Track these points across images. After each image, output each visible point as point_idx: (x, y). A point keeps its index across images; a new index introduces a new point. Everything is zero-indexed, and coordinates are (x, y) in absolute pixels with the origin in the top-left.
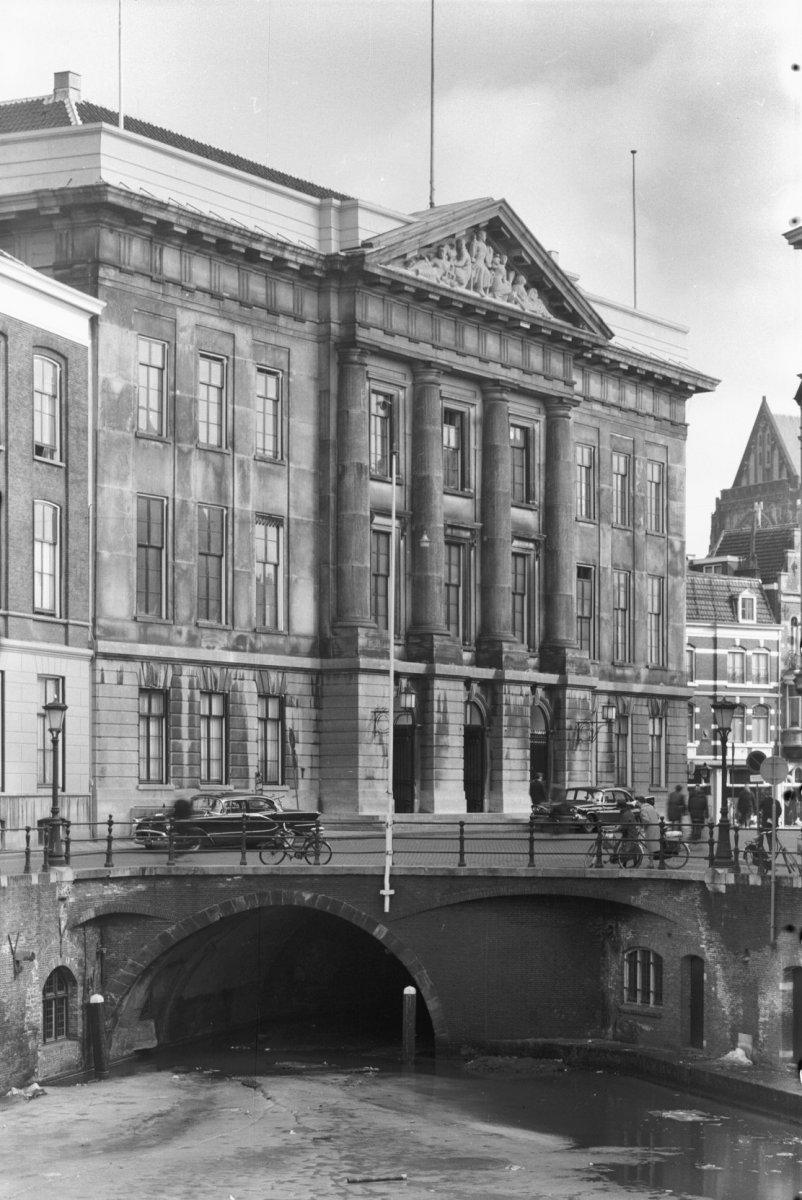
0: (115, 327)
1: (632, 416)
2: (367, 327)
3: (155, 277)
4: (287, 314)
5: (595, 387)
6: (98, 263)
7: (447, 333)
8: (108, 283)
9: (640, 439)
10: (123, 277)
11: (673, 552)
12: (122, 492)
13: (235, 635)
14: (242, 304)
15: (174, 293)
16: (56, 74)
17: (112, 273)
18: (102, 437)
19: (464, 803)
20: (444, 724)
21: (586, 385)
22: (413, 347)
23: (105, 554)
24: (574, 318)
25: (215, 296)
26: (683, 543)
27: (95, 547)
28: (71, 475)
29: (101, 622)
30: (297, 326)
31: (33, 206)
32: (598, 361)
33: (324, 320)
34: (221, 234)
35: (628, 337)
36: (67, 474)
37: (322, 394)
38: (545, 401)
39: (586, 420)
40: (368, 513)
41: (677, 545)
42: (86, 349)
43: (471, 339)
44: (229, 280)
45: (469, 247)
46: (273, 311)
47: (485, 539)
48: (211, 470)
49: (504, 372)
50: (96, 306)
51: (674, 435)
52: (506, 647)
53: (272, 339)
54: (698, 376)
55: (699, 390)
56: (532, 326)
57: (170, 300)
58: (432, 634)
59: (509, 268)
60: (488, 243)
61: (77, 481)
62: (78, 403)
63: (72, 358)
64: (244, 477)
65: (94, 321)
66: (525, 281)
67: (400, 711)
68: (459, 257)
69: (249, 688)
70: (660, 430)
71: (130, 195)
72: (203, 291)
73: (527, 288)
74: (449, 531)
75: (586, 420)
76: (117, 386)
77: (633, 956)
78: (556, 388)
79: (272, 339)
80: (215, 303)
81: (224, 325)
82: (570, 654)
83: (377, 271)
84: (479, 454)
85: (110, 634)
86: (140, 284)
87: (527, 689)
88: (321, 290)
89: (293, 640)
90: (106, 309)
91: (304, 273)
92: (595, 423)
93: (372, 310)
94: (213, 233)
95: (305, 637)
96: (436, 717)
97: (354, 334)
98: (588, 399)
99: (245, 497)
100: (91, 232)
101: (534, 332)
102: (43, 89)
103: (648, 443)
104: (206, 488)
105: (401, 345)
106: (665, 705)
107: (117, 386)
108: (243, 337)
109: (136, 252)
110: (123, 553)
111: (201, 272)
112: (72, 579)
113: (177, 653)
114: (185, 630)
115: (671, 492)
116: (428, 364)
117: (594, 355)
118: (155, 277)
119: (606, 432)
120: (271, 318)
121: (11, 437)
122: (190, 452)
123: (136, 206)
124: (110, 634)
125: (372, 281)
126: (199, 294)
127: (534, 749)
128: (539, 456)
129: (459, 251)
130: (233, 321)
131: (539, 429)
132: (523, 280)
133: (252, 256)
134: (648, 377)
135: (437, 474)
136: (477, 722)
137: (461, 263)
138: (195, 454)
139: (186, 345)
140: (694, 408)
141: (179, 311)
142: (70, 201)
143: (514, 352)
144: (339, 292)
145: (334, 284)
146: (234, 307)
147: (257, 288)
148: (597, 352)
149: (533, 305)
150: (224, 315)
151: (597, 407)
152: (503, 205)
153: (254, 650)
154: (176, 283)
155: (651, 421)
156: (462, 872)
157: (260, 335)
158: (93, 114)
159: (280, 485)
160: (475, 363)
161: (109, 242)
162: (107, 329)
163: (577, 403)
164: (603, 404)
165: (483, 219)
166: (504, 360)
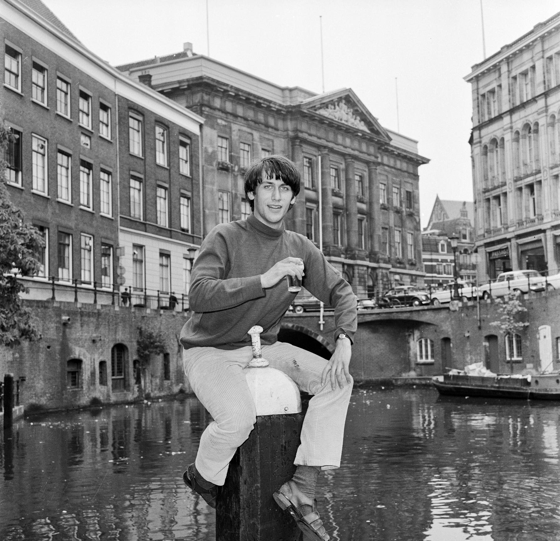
1: (399, 172)
4: (272, 128)
5: (386, 160)
7: (331, 136)
8: (206, 113)
10: (211, 111)
11: (417, 222)
12: (213, 189)
15: (231, 118)
17: (207, 109)
18: (205, 168)
21: (382, 159)
23: (207, 211)
24: (377, 133)
25: (246, 119)
26: (419, 219)
27: (203, 208)
28: (194, 181)
30: (276, 132)
31: (177, 86)
32: (386, 150)
34: (247, 96)
39: (383, 172)
41: (418, 220)
42: (198, 136)
43: (340, 139)
44: (250, 114)
45: (338, 105)
46: (267, 126)
50: (202, 120)
53: (267, 136)
54: (423, 158)
55: (424, 163)
56: (363, 135)
59: (353, 114)
60: (345, 104)
62: (195, 155)
63: (193, 138)
65: (201, 126)
68: (335, 108)
70: (409, 177)
72: (241, 117)
73: (360, 121)
74: (334, 210)
75: (383, 172)
76: (210, 150)
79: (267, 136)
80: (245, 122)
81: (249, 130)
83: (305, 111)
84: (344, 182)
87: (365, 268)
88: (284, 120)
90: (205, 122)
91: (278, 112)
92: (386, 173)
93: (304, 127)
94: (245, 95)
101: (364, 137)
102: (181, 50)
103: (405, 182)
105: (314, 139)
106: (416, 279)
107: (210, 150)
108: (256, 135)
110: (214, 211)
111: (240, 111)
116: (325, 147)
117: (385, 148)
120: (266, 129)
121: (171, 164)
122: (237, 175)
123: (215, 84)
126: (239, 119)
128: (366, 184)
129: (335, 106)
130: (252, 129)
131: (366, 174)
132: (358, 118)
133: (258, 105)
134: (405, 157)
137: (336, 111)
139: (235, 136)
140: (422, 170)
142: (191, 83)
143: (356, 145)
144: (291, 120)
145: (289, 117)
146: (252, 123)
147: (261, 117)
148: (386, 147)
149: (362, 127)
150: (249, 127)
151: (386, 168)
152: (350, 90)
154: (232, 114)
155: (406, 174)
157: (262, 134)
160: (342, 148)
162: (206, 129)
164: (388, 166)
165: (343, 95)
166: (353, 147)
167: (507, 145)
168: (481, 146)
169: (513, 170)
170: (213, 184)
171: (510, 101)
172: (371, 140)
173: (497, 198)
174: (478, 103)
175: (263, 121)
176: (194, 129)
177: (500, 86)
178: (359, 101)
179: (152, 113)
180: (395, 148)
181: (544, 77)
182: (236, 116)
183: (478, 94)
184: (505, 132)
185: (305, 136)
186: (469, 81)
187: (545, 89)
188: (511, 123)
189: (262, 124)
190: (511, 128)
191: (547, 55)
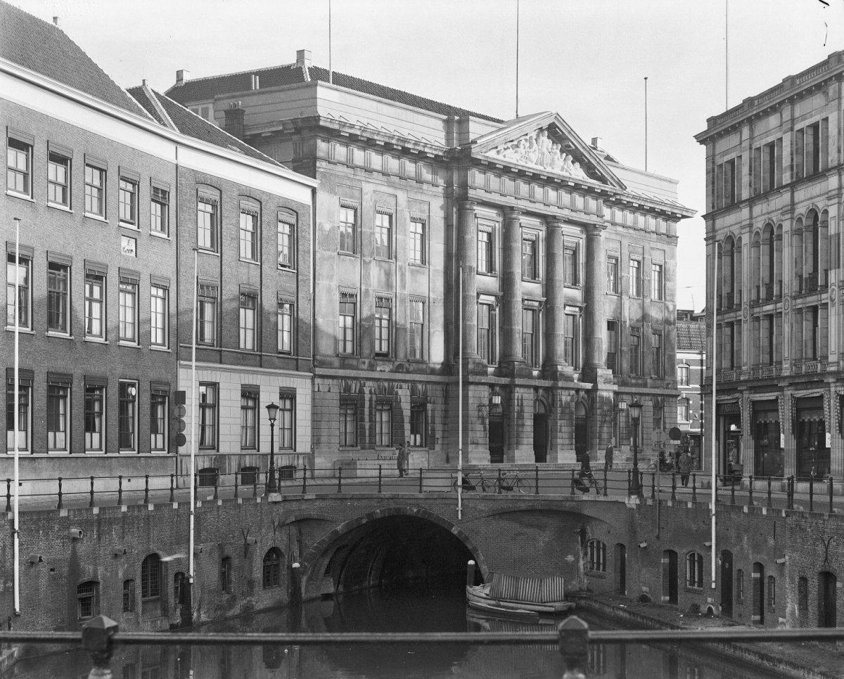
0: (326, 194)
1: (643, 233)
3: (349, 164)
8: (322, 170)
10: (331, 166)
11: (668, 311)
12: (330, 286)
13: (397, 363)
15: (361, 175)
16: (297, 52)
17: (324, 164)
18: (318, 255)
19: (533, 457)
20: (521, 412)
22: (503, 199)
24: (602, 179)
28: (300, 277)
29: (318, 357)
30: (434, 189)
33: (449, 184)
34: (387, 140)
35: (636, 187)
36: (297, 276)
37: (448, 227)
38: (585, 227)
39: (613, 237)
40: (475, 294)
41: (671, 308)
44: (393, 164)
47: (548, 306)
48: (382, 271)
49: (559, 211)
51: (669, 243)
52: (559, 368)
53: (419, 197)
55: (684, 217)
56: (576, 184)
57: (358, 178)
58: (514, 362)
59: (562, 151)
60: (549, 137)
62: (304, 237)
64: (403, 275)
65: (314, 191)
66: (572, 159)
67: (492, 405)
69: (404, 394)
71: (332, 121)
73: (573, 162)
75: (613, 237)
77: (592, 543)
78: (592, 219)
79: (419, 197)
80: (385, 178)
81: (391, 191)
82: (600, 372)
83: (479, 157)
85: (323, 364)
86: (341, 169)
87: (573, 392)
92: (618, 238)
93: (477, 178)
96: (516, 408)
97: (467, 193)
98: (614, 224)
99: (404, 287)
100: (312, 142)
101: (577, 188)
102: (291, 60)
103: (652, 248)
104: (379, 282)
106: (663, 401)
107: (327, 227)
108: (402, 197)
109: (340, 151)
110: (331, 319)
111: (376, 160)
112: (300, 334)
113: (363, 374)
114: (367, 361)
115: (667, 276)
116: (512, 208)
117: (616, 199)
118: (349, 164)
119: (625, 242)
122: (370, 262)
123: (336, 127)
124: (323, 364)
125: (476, 163)
127: (577, 427)
128: (582, 258)
131: (582, 243)
132: (571, 158)
134: (652, 210)
135: (517, 270)
136: (542, 411)
138: (373, 263)
141: (363, 184)
146: (397, 179)
147: (410, 167)
148: (618, 197)
149: (577, 173)
150: (391, 185)
151: (620, 229)
153: (408, 372)
155: (655, 235)
157: (412, 195)
158: (319, 74)
159: (423, 279)
160: (542, 206)
161: (322, 147)
163: (605, 228)
165: (545, 124)
167: (745, 251)
169: (750, 290)
170: (331, 277)
171: (750, 186)
172: (590, 191)
174: (713, 178)
175: (413, 175)
176: (304, 196)
177: (740, 157)
178: (571, 131)
179: (234, 184)
180: (634, 197)
181: (792, 160)
182: (368, 170)
183: (713, 163)
184: (744, 231)
186: (702, 142)
187: (792, 178)
188: (751, 218)
190: (751, 225)
191: (798, 127)
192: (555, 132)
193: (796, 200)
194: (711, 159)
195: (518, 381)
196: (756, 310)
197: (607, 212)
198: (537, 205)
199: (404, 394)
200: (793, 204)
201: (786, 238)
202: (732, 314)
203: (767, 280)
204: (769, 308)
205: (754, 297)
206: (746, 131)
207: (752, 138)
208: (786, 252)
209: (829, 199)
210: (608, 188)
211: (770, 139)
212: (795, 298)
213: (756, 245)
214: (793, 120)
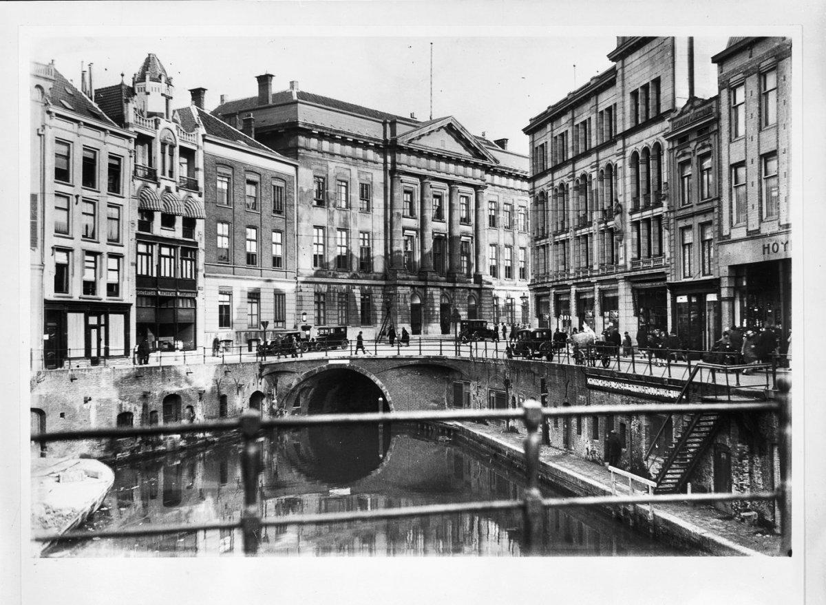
2: (400, 164)
6: (298, 147)
9: (516, 198)
10: (307, 152)
13: (351, 273)
14: (353, 158)
15: (327, 157)
17: (303, 151)
19: (440, 331)
22: (419, 170)
24: (484, 158)
25: (343, 156)
30: (376, 165)
33: (385, 163)
38: (477, 188)
40: (401, 230)
44: (348, 149)
46: (366, 161)
49: (456, 177)
53: (365, 170)
57: (325, 159)
58: (426, 272)
61: (290, 223)
65: (296, 167)
69: (357, 292)
75: (494, 193)
76: (305, 190)
78: (478, 182)
79: (365, 170)
80: (342, 159)
81: (347, 166)
86: (314, 154)
89: (374, 275)
92: (497, 193)
93: (403, 158)
95: (379, 273)
105: (414, 170)
109: (314, 142)
111: (337, 148)
112: (288, 256)
119: (501, 196)
120: (365, 163)
121: (263, 209)
128: (472, 206)
131: (473, 197)
138: (336, 211)
146: (351, 160)
147: (359, 152)
153: (359, 278)
156: (398, 357)
158: (302, 95)
160: (445, 175)
161: (302, 140)
167: (550, 200)
168: (534, 196)
172: (475, 166)
173: (543, 247)
177: (546, 142)
178: (463, 128)
182: (333, 154)
185: (405, 168)
186: (527, 133)
189: (361, 159)
190: (552, 185)
192: (452, 130)
193: (576, 169)
194: (533, 142)
195: (429, 283)
196: (557, 237)
197: (488, 177)
198: (442, 174)
199: (357, 292)
200: (574, 171)
201: (571, 192)
202: (544, 241)
203: (561, 219)
204: (563, 236)
205: (555, 230)
206: (549, 127)
207: (552, 130)
208: (571, 202)
209: (592, 167)
210: (485, 162)
211: (562, 131)
212: (576, 230)
213: (555, 197)
214: (573, 119)
